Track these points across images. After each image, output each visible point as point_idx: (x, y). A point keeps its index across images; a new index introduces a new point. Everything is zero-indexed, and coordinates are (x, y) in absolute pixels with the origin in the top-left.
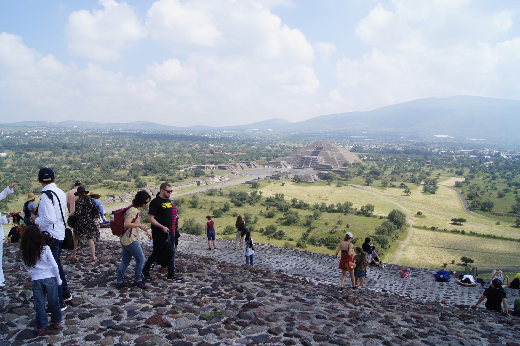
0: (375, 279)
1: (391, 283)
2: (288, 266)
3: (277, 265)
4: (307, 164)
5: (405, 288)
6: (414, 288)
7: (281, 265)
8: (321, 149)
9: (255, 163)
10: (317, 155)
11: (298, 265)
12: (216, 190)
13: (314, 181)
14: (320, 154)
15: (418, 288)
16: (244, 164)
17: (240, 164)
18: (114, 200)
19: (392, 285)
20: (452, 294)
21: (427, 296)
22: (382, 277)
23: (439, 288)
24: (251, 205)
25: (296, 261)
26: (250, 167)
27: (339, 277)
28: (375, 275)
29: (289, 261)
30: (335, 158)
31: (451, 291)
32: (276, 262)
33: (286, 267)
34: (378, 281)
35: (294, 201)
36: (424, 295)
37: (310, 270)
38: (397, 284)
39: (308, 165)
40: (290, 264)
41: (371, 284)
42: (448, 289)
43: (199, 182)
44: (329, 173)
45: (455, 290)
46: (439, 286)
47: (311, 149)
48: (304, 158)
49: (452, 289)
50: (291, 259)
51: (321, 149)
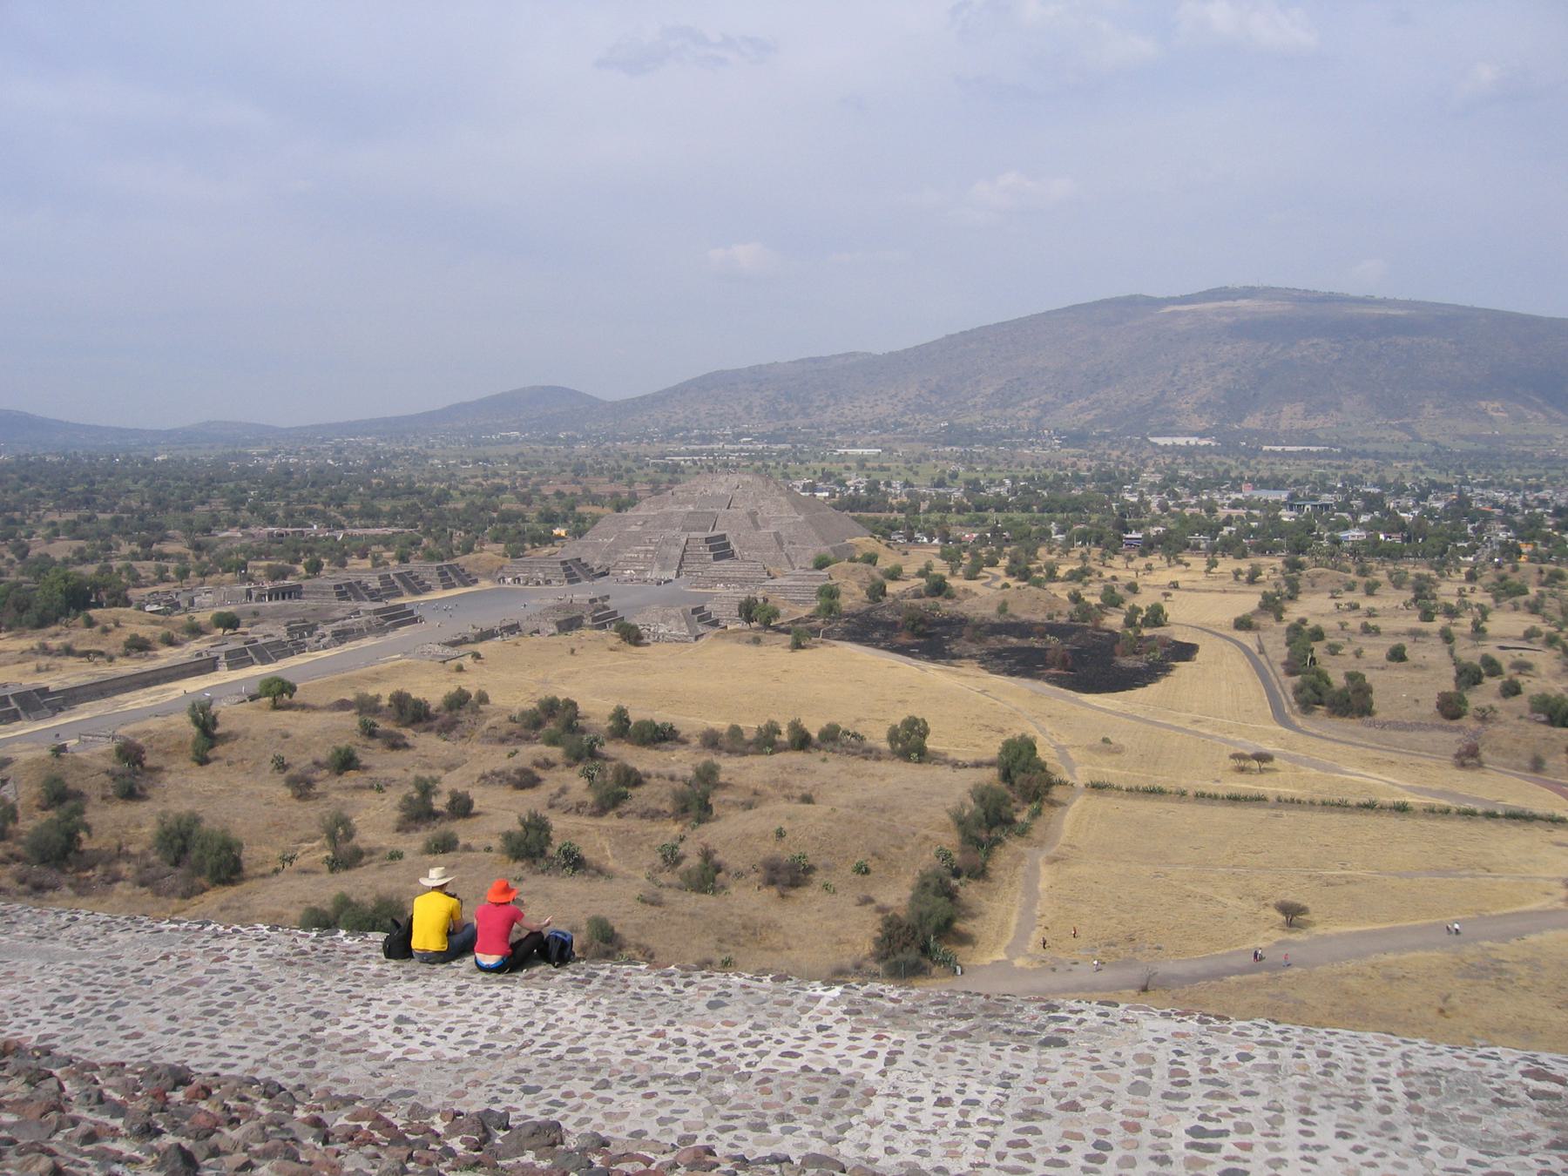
0: (871, 1076)
1: (944, 1093)
2: (455, 1037)
3: (398, 1038)
5: (1010, 1110)
6: (1050, 1105)
7: (422, 1037)
11: (506, 1028)
15: (1073, 1106)
19: (944, 1102)
20: (1227, 1124)
21: (1109, 1147)
22: (902, 1062)
23: (1166, 1096)
25: (498, 1012)
27: (692, 1077)
28: (872, 1055)
29: (466, 1009)
31: (1224, 1106)
32: (402, 1019)
33: (441, 1047)
34: (883, 1088)
35: (620, 716)
36: (1097, 1145)
37: (555, 1052)
38: (971, 1094)
40: (462, 1029)
41: (850, 1103)
42: (1209, 1095)
45: (1244, 1102)
46: (1168, 1087)
49: (1223, 1096)
50: (476, 1002)
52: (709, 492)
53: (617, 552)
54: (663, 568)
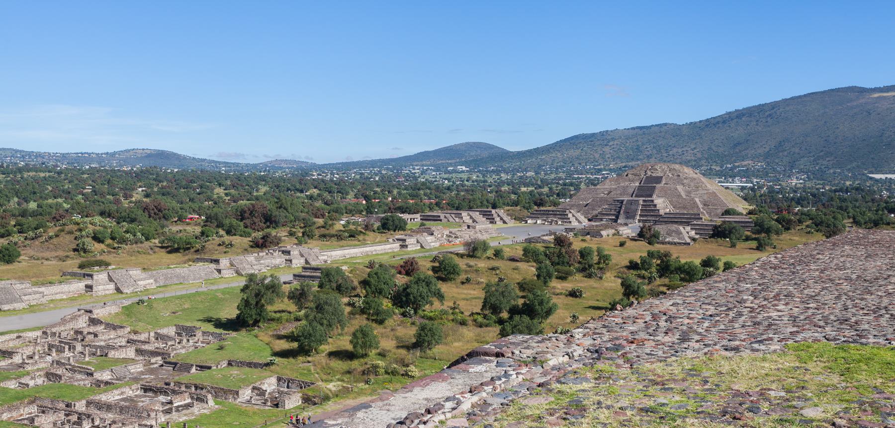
4: (630, 215)
8: (658, 180)
9: (501, 212)
10: (651, 196)
12: (485, 246)
13: (688, 240)
14: (657, 192)
16: (478, 213)
17: (471, 213)
18: (219, 271)
24: (590, 276)
26: (493, 221)
30: (697, 200)
39: (633, 217)
43: (404, 240)
44: (724, 222)
47: (633, 181)
48: (622, 202)
51: (658, 180)
52: (649, 173)
53: (593, 209)
54: (627, 218)
